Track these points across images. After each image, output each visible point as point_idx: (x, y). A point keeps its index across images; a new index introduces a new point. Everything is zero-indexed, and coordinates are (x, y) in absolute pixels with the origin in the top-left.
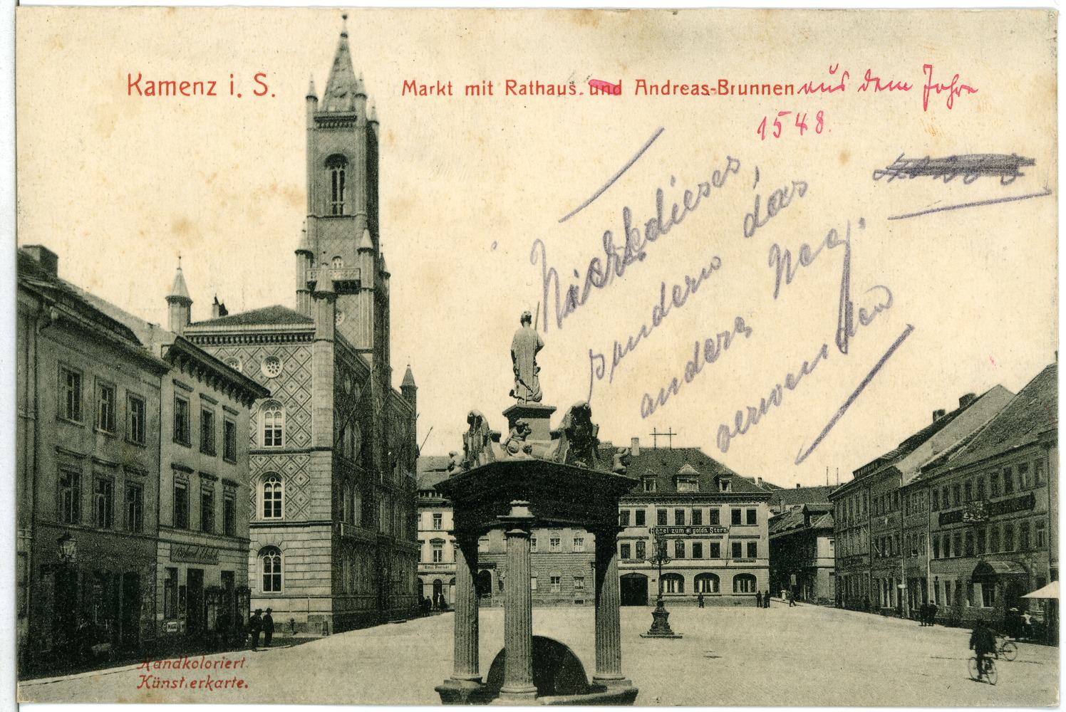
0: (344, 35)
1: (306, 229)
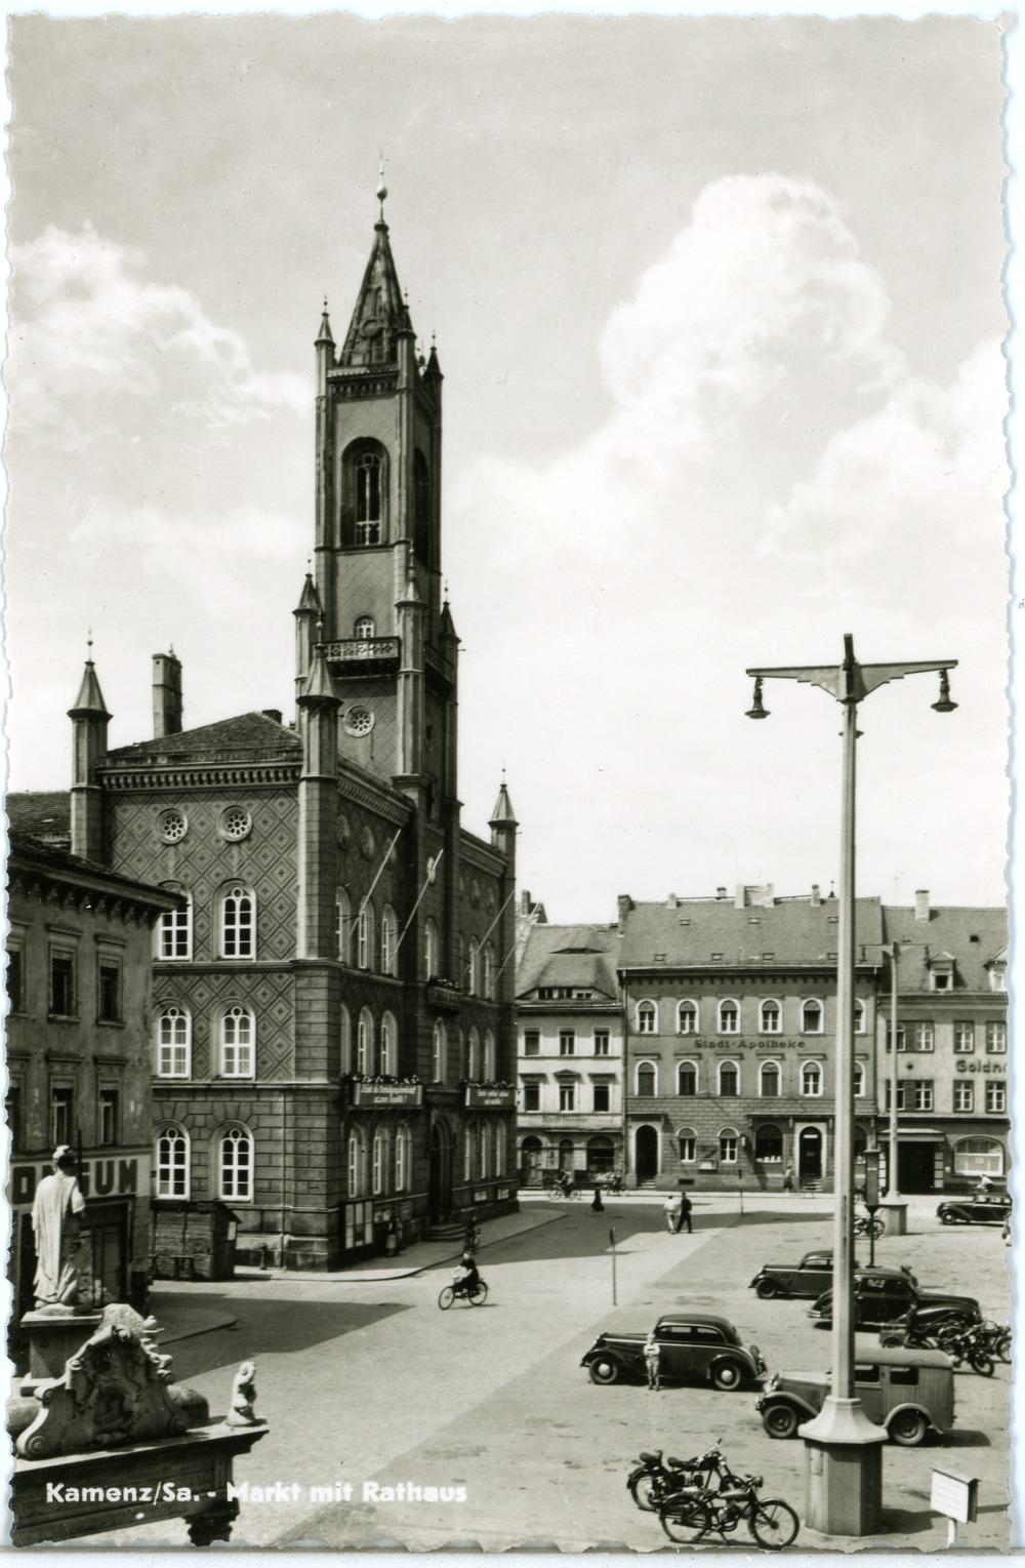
0: (382, 228)
1: (313, 573)
